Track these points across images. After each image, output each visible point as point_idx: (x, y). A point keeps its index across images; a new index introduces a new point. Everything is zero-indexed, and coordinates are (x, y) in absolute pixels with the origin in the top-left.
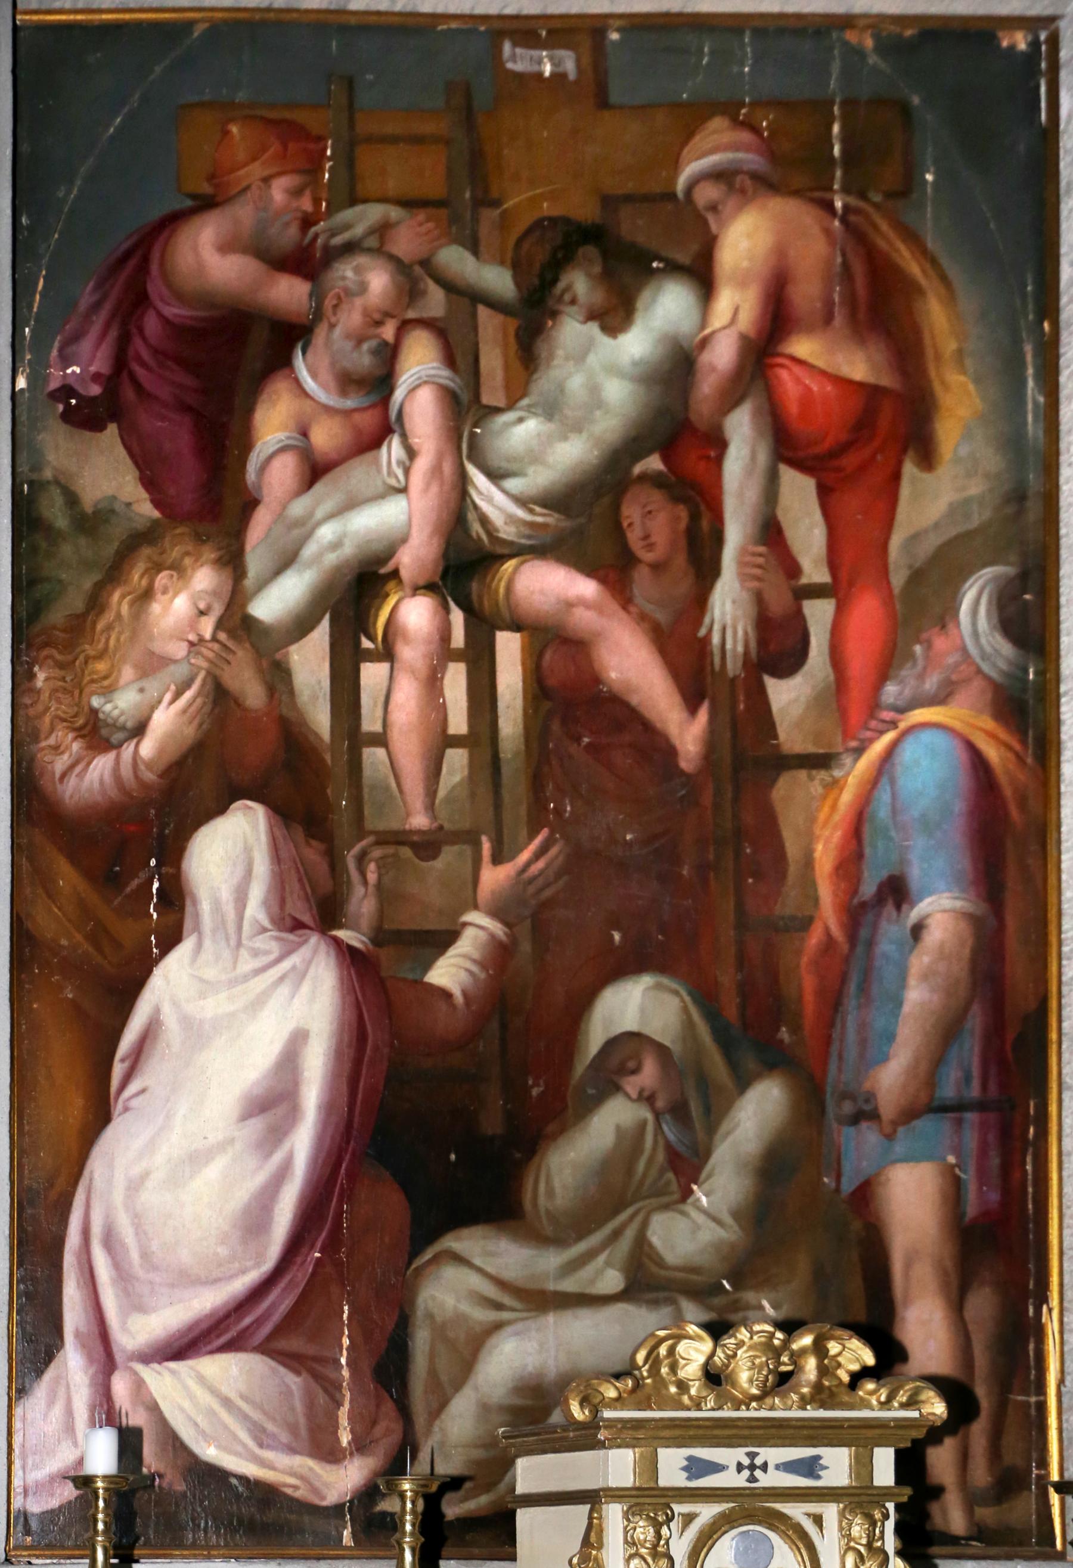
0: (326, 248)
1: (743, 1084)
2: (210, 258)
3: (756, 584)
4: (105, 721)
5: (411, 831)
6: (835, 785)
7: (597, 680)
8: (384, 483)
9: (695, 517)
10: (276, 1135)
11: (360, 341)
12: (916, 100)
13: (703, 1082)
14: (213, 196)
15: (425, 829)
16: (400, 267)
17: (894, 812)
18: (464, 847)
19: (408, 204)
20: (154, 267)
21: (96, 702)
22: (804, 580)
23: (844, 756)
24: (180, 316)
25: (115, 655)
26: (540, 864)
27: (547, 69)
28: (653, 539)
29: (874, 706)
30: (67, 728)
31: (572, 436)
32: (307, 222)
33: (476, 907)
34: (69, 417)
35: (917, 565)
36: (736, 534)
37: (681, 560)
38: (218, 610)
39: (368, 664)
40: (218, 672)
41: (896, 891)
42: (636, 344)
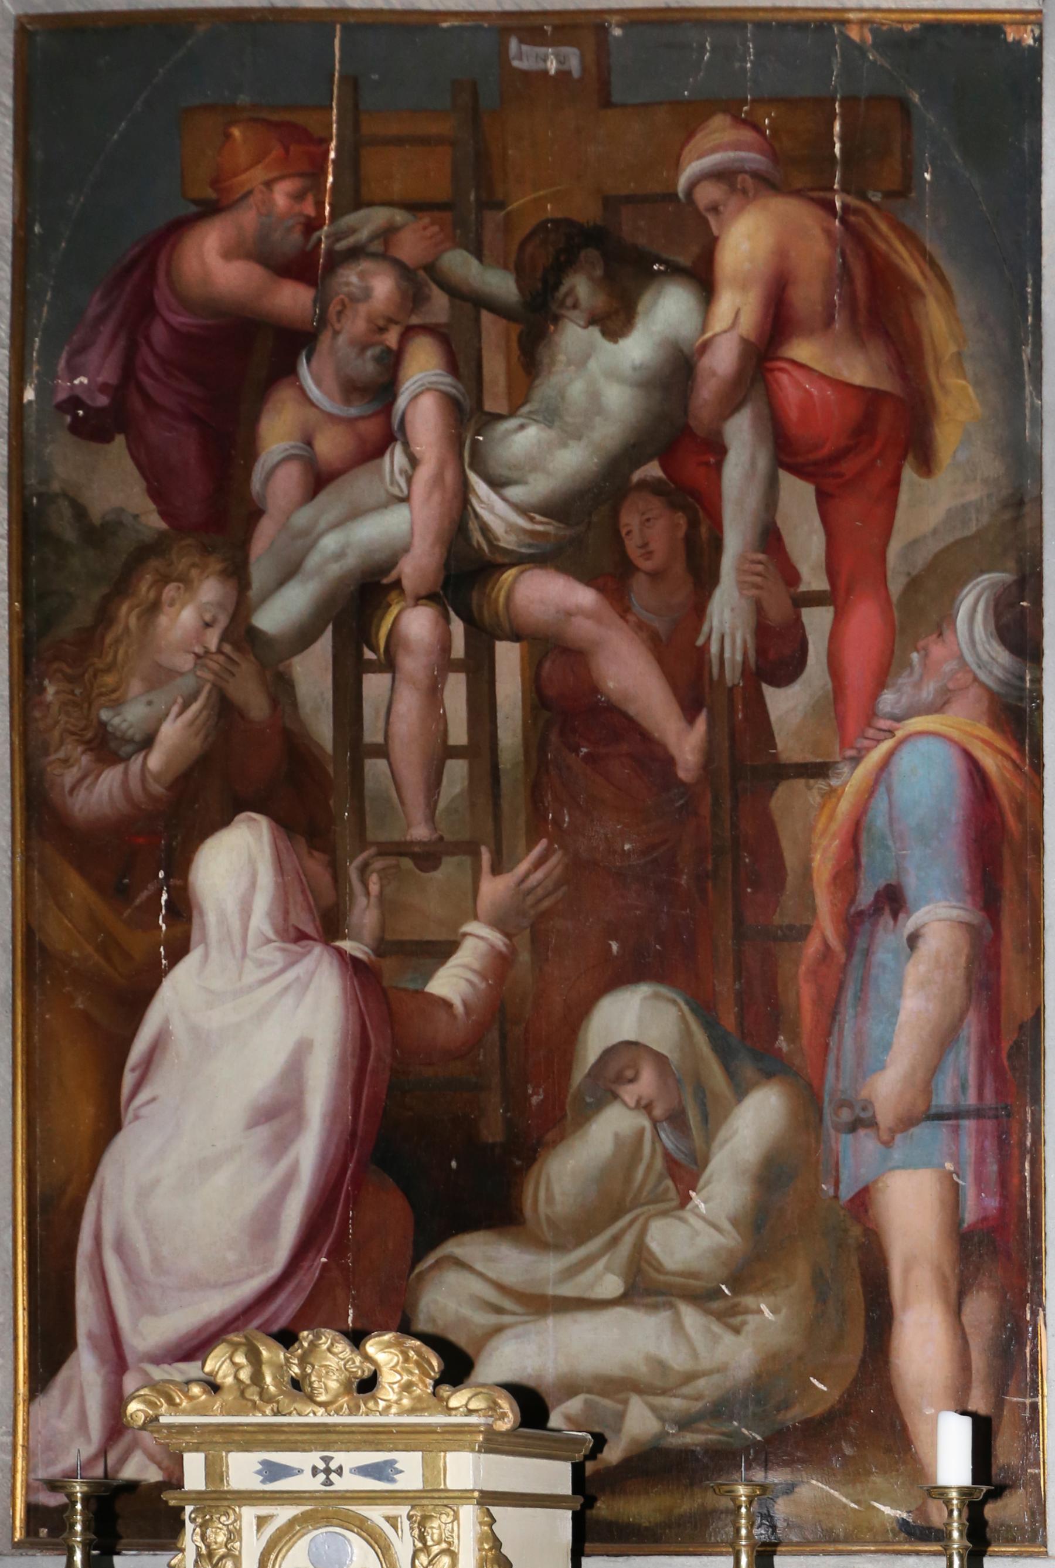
0: (330, 252)
1: (741, 1092)
2: (214, 263)
3: (754, 592)
5: (412, 843)
6: (832, 794)
7: (595, 690)
8: (387, 491)
9: (693, 524)
10: (281, 1143)
11: (364, 348)
12: (916, 98)
13: (701, 1091)
15: (426, 840)
16: (404, 271)
17: (891, 821)
18: (464, 858)
19: (413, 207)
21: (105, 715)
22: (803, 588)
23: (840, 766)
24: (183, 324)
25: (123, 667)
26: (539, 875)
27: (552, 66)
29: (871, 714)
30: (77, 740)
31: (571, 443)
33: (476, 917)
34: (77, 428)
35: (914, 573)
36: (736, 539)
37: (679, 568)
38: (223, 621)
39: (370, 675)
41: (893, 900)
42: (637, 348)
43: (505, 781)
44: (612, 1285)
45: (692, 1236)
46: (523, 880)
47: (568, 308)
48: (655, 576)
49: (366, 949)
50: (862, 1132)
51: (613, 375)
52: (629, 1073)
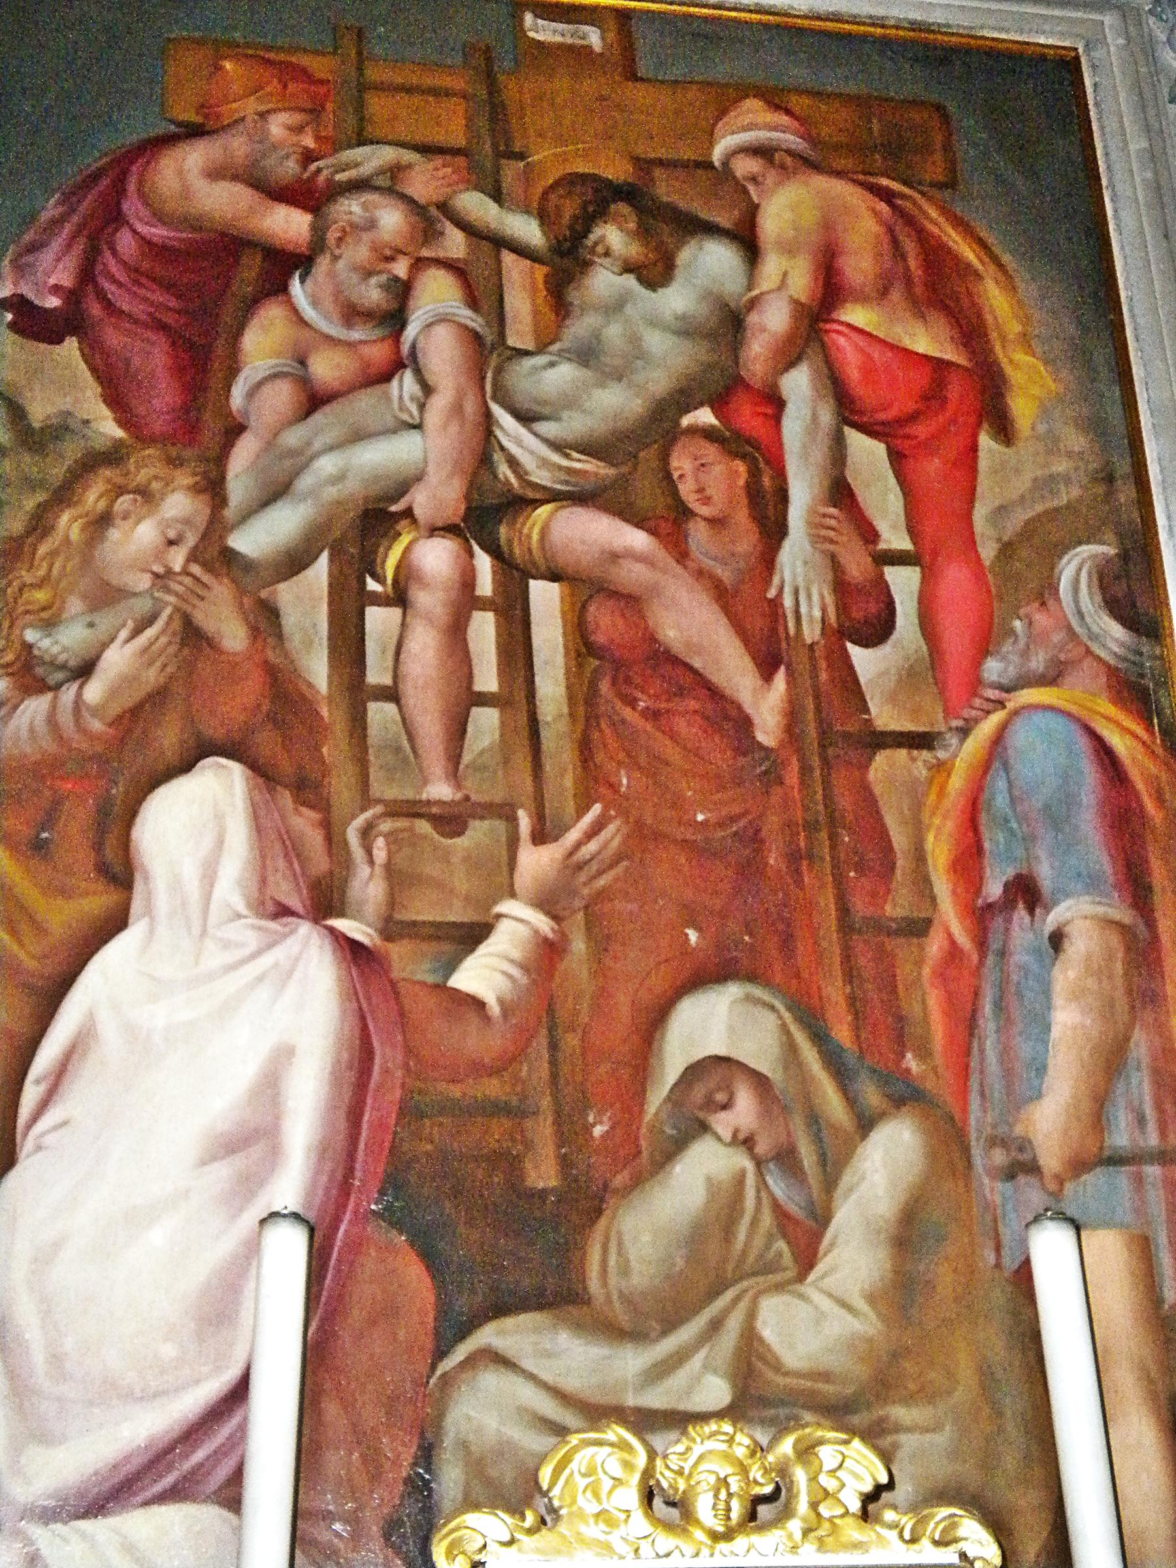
0: (330, 181)
1: (866, 1124)
4: (41, 658)
5: (428, 803)
6: (941, 768)
9: (754, 474)
10: (249, 1185)
14: (203, 125)
17: (1013, 801)
19: (426, 150)
20: (132, 187)
21: (30, 636)
22: (882, 546)
26: (592, 846)
28: (708, 492)
29: (975, 683)
32: (308, 157)
33: (513, 895)
35: (1006, 539)
36: (803, 492)
37: (742, 516)
38: (191, 540)
40: (189, 609)
43: (546, 735)
44: (716, 1391)
45: (814, 1324)
46: (571, 854)
47: (599, 257)
48: (712, 522)
49: (370, 931)
50: (1022, 1179)
51: (654, 322)
52: (720, 1097)
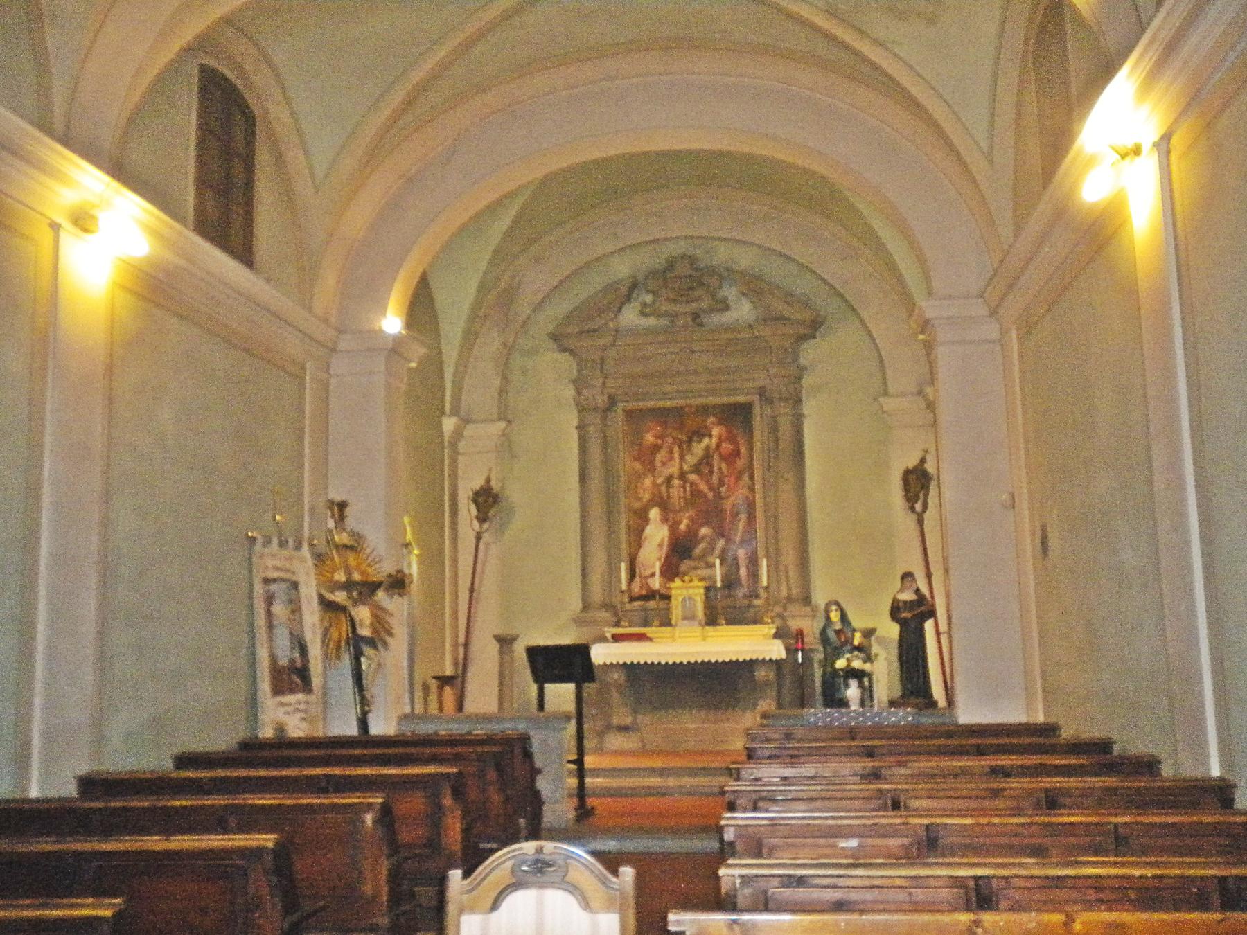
41: (737, 514)
